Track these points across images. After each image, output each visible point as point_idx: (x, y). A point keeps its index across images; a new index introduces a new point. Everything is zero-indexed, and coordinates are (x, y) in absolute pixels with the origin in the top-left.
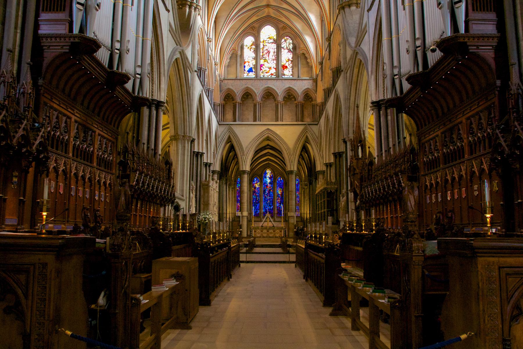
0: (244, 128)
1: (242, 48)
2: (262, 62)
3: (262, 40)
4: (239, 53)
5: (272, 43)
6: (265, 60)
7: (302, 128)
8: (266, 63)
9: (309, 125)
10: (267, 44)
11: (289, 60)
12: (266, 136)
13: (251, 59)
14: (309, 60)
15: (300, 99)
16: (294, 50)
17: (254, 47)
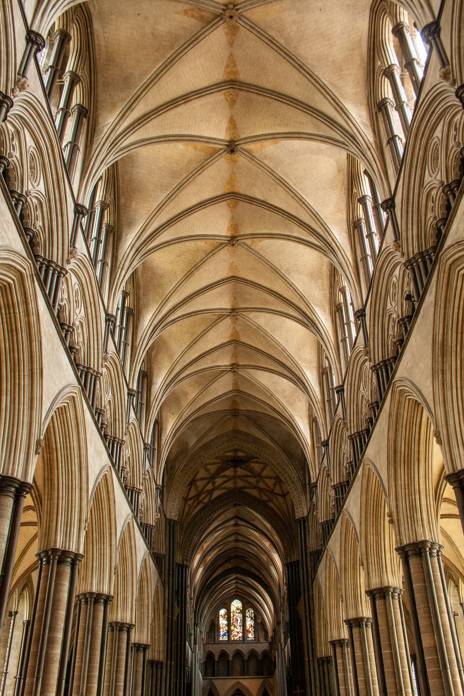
0: (220, 681)
1: (218, 618)
2: (232, 628)
3: (232, 611)
4: (216, 622)
5: (239, 613)
6: (235, 626)
7: (262, 680)
8: (235, 629)
9: (267, 678)
10: (236, 614)
11: (251, 626)
12: (236, 688)
13: (224, 625)
14: (265, 627)
15: (260, 658)
16: (255, 619)
17: (226, 616)
